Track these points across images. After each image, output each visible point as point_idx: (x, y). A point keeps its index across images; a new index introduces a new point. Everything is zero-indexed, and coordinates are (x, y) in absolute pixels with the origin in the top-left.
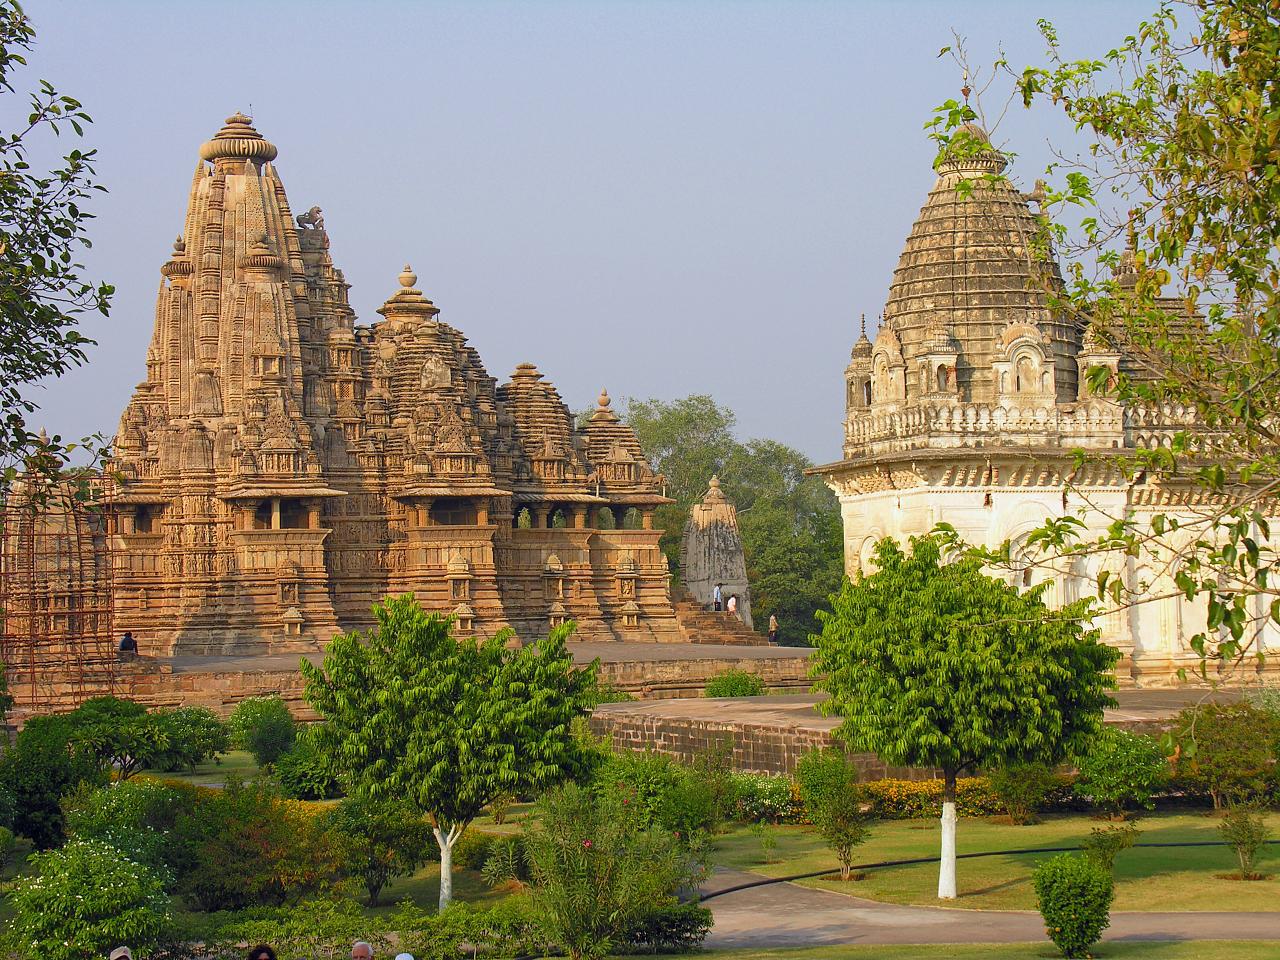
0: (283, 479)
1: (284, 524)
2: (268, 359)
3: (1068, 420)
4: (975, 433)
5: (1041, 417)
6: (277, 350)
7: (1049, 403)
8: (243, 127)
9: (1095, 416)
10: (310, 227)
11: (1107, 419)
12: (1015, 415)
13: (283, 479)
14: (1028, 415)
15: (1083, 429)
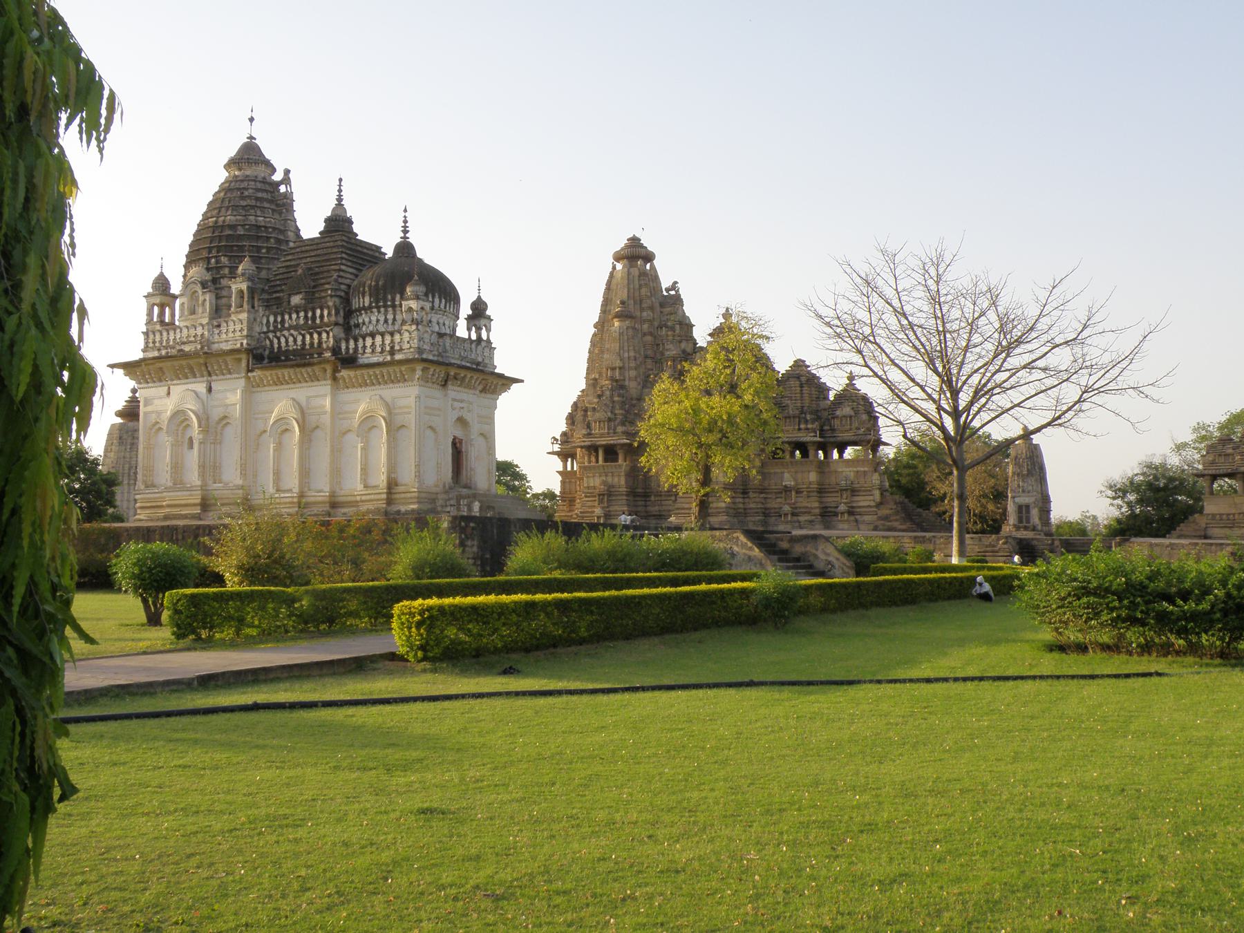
0: (602, 435)
1: (606, 460)
2: (613, 369)
3: (216, 331)
4: (166, 348)
5: (199, 331)
6: (618, 363)
7: (205, 321)
8: (635, 242)
9: (231, 328)
10: (673, 293)
11: (238, 327)
12: (185, 331)
13: (602, 435)
14: (192, 332)
15: (224, 336)
